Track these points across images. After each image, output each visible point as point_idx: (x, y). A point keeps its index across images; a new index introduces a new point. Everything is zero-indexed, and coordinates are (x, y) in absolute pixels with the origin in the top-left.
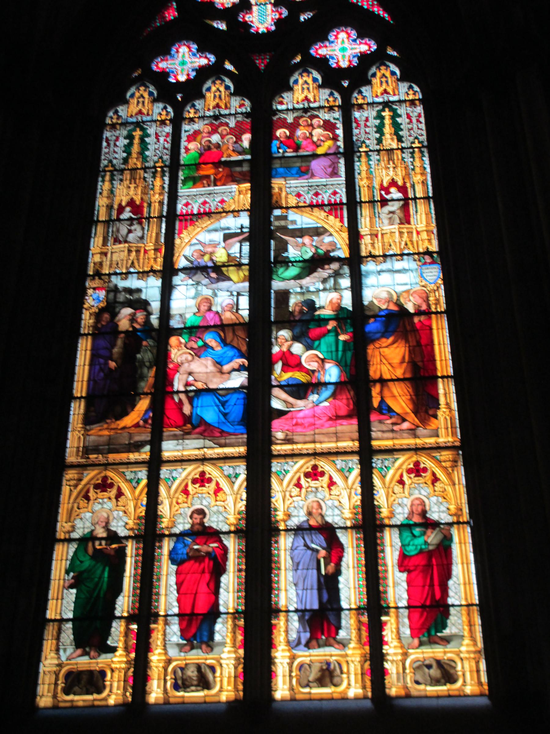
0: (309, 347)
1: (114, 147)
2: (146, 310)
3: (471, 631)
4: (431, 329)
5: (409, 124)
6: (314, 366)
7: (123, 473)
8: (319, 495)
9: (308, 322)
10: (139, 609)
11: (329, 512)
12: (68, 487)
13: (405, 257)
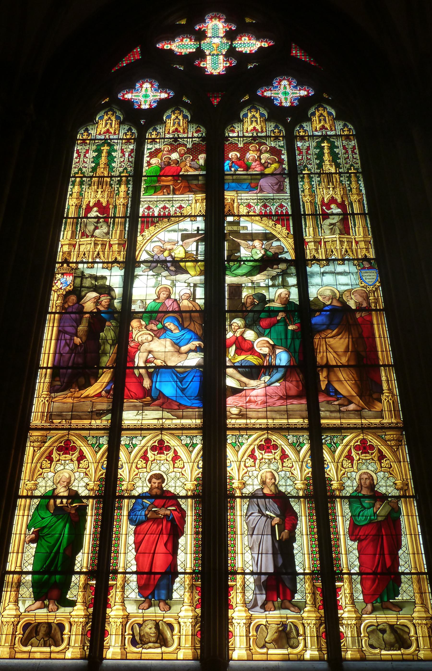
0: (260, 335)
1: (83, 159)
2: (109, 294)
3: (421, 597)
4: (372, 324)
5: (345, 154)
6: (265, 350)
7: (86, 437)
8: (272, 466)
9: (260, 312)
10: (98, 565)
11: (282, 482)
12: (32, 448)
13: (346, 262)
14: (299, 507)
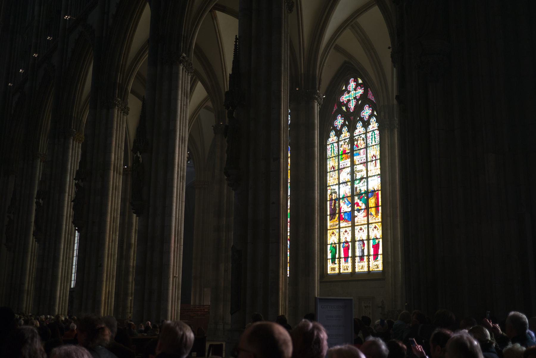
14: (366, 242)
